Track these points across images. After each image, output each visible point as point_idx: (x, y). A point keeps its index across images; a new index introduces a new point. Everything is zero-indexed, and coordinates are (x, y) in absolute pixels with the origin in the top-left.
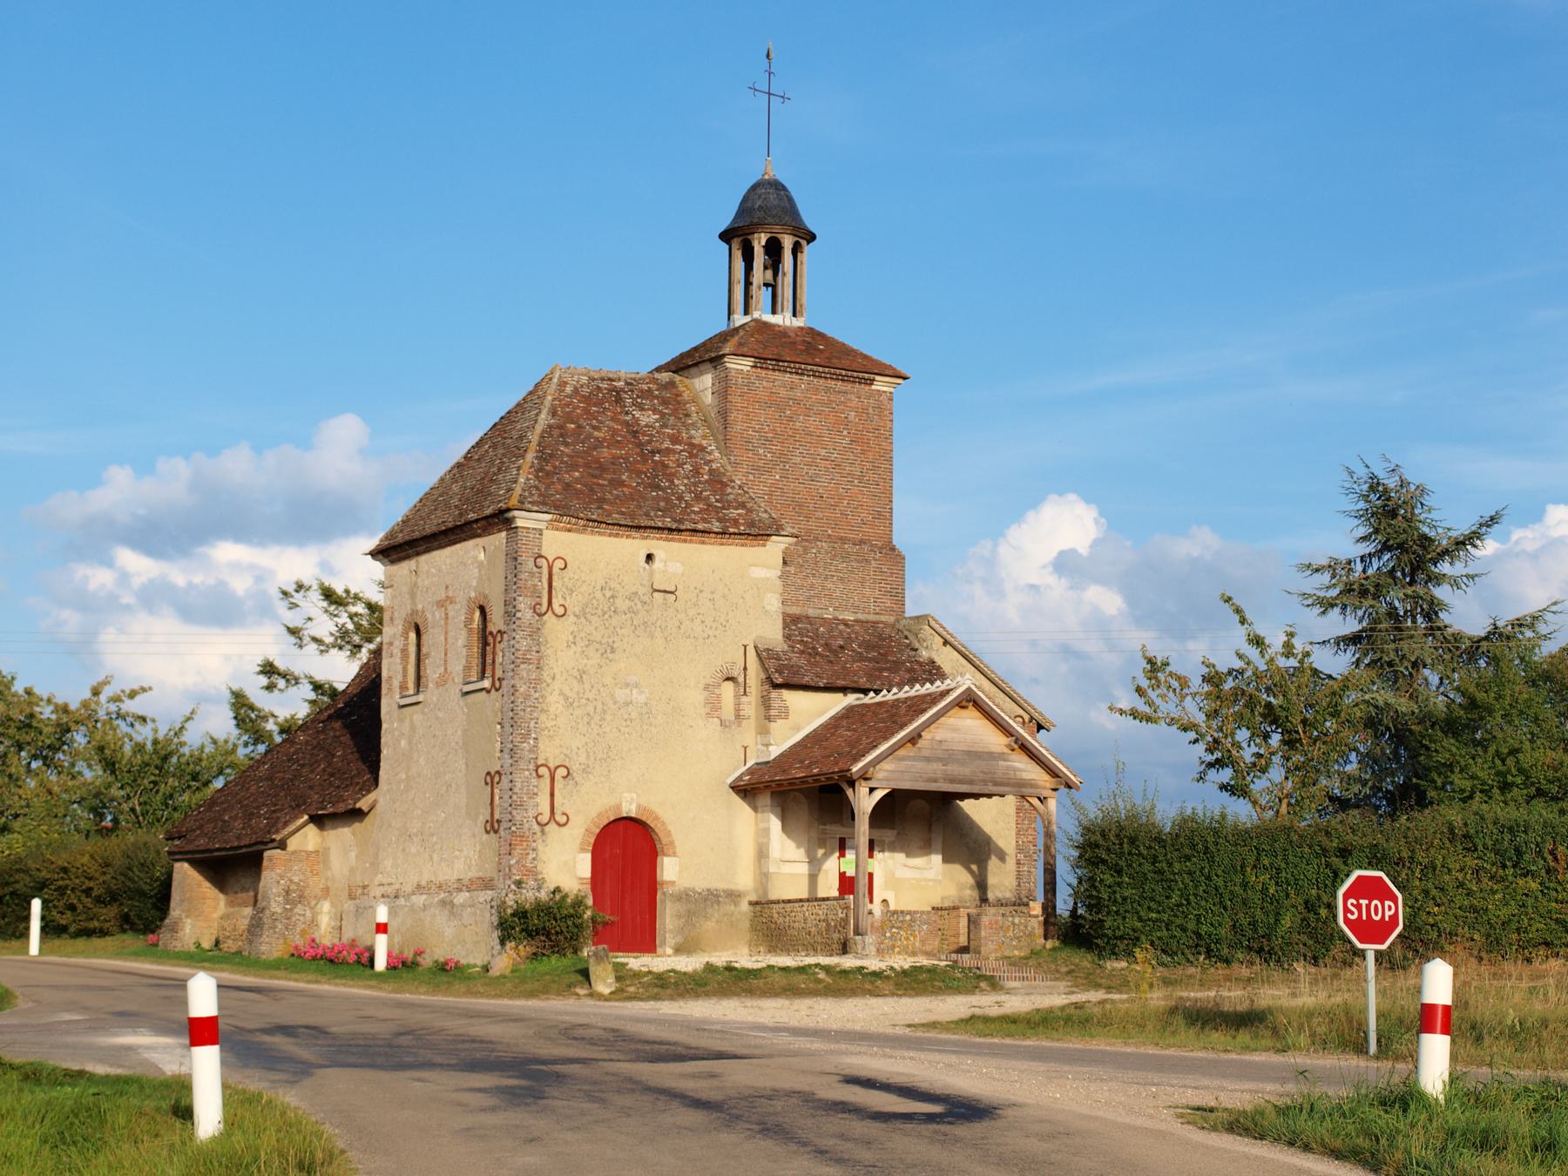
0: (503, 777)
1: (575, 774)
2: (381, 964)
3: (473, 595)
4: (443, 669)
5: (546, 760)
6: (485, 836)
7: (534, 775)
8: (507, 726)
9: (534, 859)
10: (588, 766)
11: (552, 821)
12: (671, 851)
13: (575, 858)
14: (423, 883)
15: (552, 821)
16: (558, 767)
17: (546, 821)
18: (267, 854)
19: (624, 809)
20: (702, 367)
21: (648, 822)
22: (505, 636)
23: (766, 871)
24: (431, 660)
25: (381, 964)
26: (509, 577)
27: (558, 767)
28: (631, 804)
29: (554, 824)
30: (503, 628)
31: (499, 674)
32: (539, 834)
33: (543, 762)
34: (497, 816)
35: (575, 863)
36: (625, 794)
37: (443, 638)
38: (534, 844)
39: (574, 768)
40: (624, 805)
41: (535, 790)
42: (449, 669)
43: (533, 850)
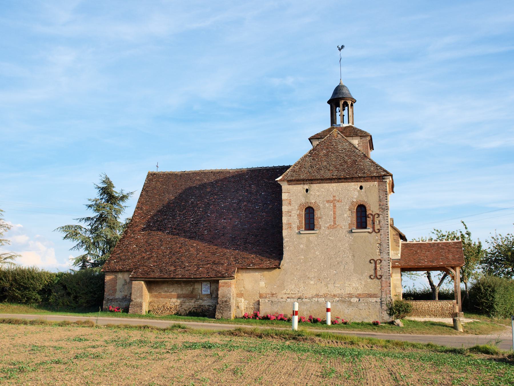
0: (383, 261)
2: (329, 323)
3: (355, 200)
4: (332, 223)
6: (369, 280)
8: (385, 245)
14: (320, 294)
18: (219, 281)
20: (354, 138)
22: (381, 216)
23: (399, 291)
24: (323, 220)
25: (329, 323)
26: (382, 197)
30: (378, 212)
31: (377, 227)
34: (379, 273)
37: (332, 213)
42: (337, 224)
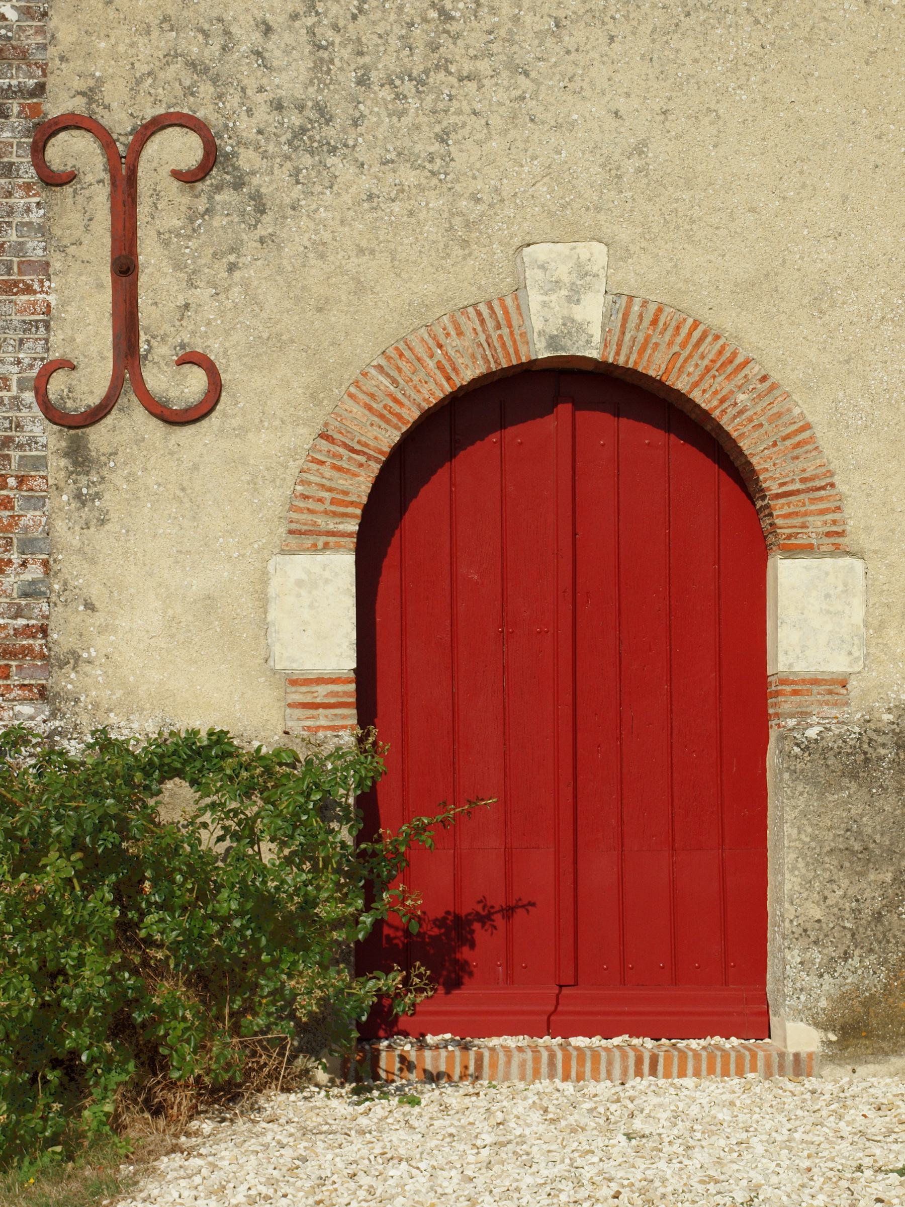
1: (247, 159)
5: (89, 95)
7: (29, 173)
9: (31, 592)
10: (324, 115)
11: (129, 399)
12: (817, 524)
13: (264, 579)
15: (129, 399)
16: (157, 125)
17: (94, 400)
19: (537, 324)
21: (681, 384)
27: (157, 125)
28: (574, 297)
29: (140, 414)
32: (57, 466)
33: (78, 105)
35: (263, 602)
36: (540, 252)
38: (30, 517)
39: (246, 127)
40: (535, 299)
41: (35, 249)
43: (27, 546)
